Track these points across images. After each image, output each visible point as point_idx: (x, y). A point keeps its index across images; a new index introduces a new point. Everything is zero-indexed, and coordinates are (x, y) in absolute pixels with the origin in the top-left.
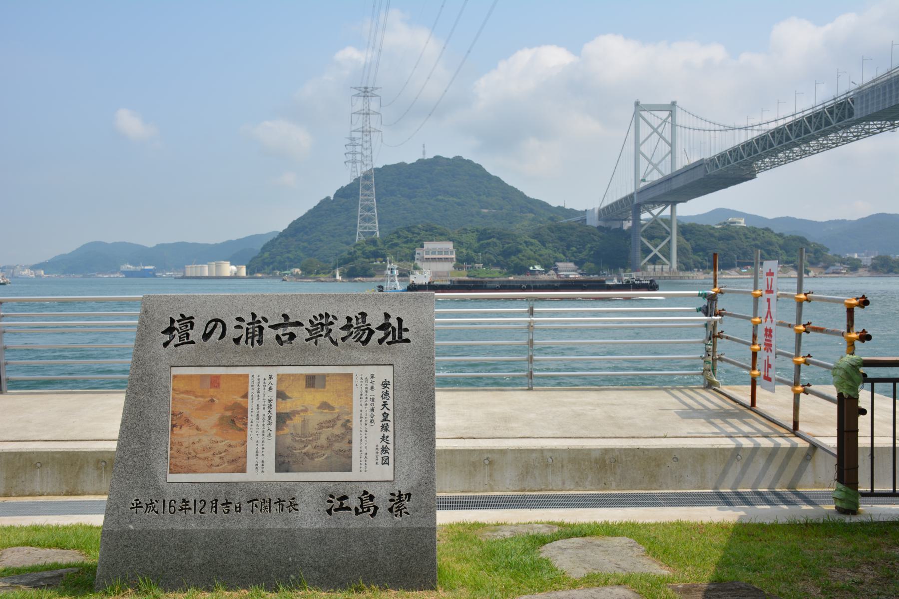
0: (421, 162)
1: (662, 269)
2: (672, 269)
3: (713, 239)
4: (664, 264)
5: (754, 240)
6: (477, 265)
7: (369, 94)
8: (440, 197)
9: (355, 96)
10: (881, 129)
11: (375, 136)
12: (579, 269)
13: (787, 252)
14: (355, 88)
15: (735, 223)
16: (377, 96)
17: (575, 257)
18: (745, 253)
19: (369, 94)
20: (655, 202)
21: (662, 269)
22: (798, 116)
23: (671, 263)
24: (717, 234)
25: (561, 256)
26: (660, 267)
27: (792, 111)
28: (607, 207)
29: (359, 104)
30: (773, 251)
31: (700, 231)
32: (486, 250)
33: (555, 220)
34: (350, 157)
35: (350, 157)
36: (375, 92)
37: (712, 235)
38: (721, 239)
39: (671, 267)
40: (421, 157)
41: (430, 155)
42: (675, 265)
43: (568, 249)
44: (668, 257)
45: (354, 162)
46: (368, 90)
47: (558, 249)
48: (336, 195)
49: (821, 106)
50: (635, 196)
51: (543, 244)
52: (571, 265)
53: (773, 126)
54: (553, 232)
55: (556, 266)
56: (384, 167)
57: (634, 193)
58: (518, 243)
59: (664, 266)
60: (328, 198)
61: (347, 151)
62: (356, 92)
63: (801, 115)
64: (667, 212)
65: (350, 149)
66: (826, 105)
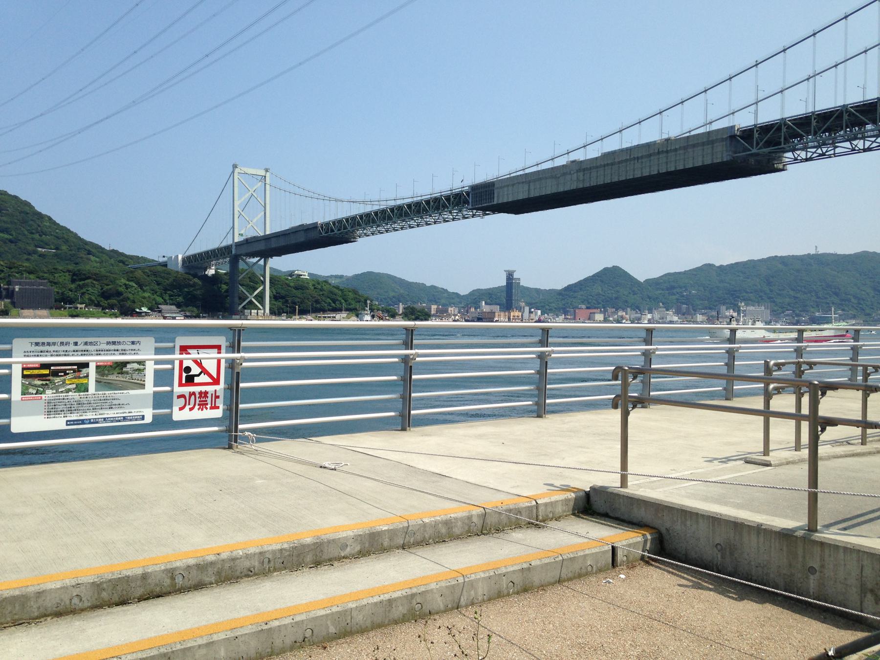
1: (257, 313)
2: (266, 314)
3: (290, 288)
4: (260, 309)
5: (321, 290)
6: (79, 306)
10: (473, 216)
12: (180, 311)
13: (346, 301)
15: (301, 275)
17: (172, 299)
18: (317, 302)
20: (253, 255)
21: (257, 313)
22: (415, 199)
24: (292, 284)
25: (160, 300)
26: (256, 311)
27: (410, 194)
28: (194, 256)
30: (337, 300)
31: (278, 281)
32: (84, 290)
33: (126, 263)
37: (289, 286)
38: (296, 288)
39: (265, 312)
43: (166, 293)
44: (262, 303)
47: (156, 293)
49: (439, 194)
50: (234, 247)
51: (141, 286)
52: (174, 307)
53: (392, 203)
54: (148, 276)
57: (231, 245)
58: (117, 285)
63: (419, 198)
64: (262, 262)
66: (442, 194)
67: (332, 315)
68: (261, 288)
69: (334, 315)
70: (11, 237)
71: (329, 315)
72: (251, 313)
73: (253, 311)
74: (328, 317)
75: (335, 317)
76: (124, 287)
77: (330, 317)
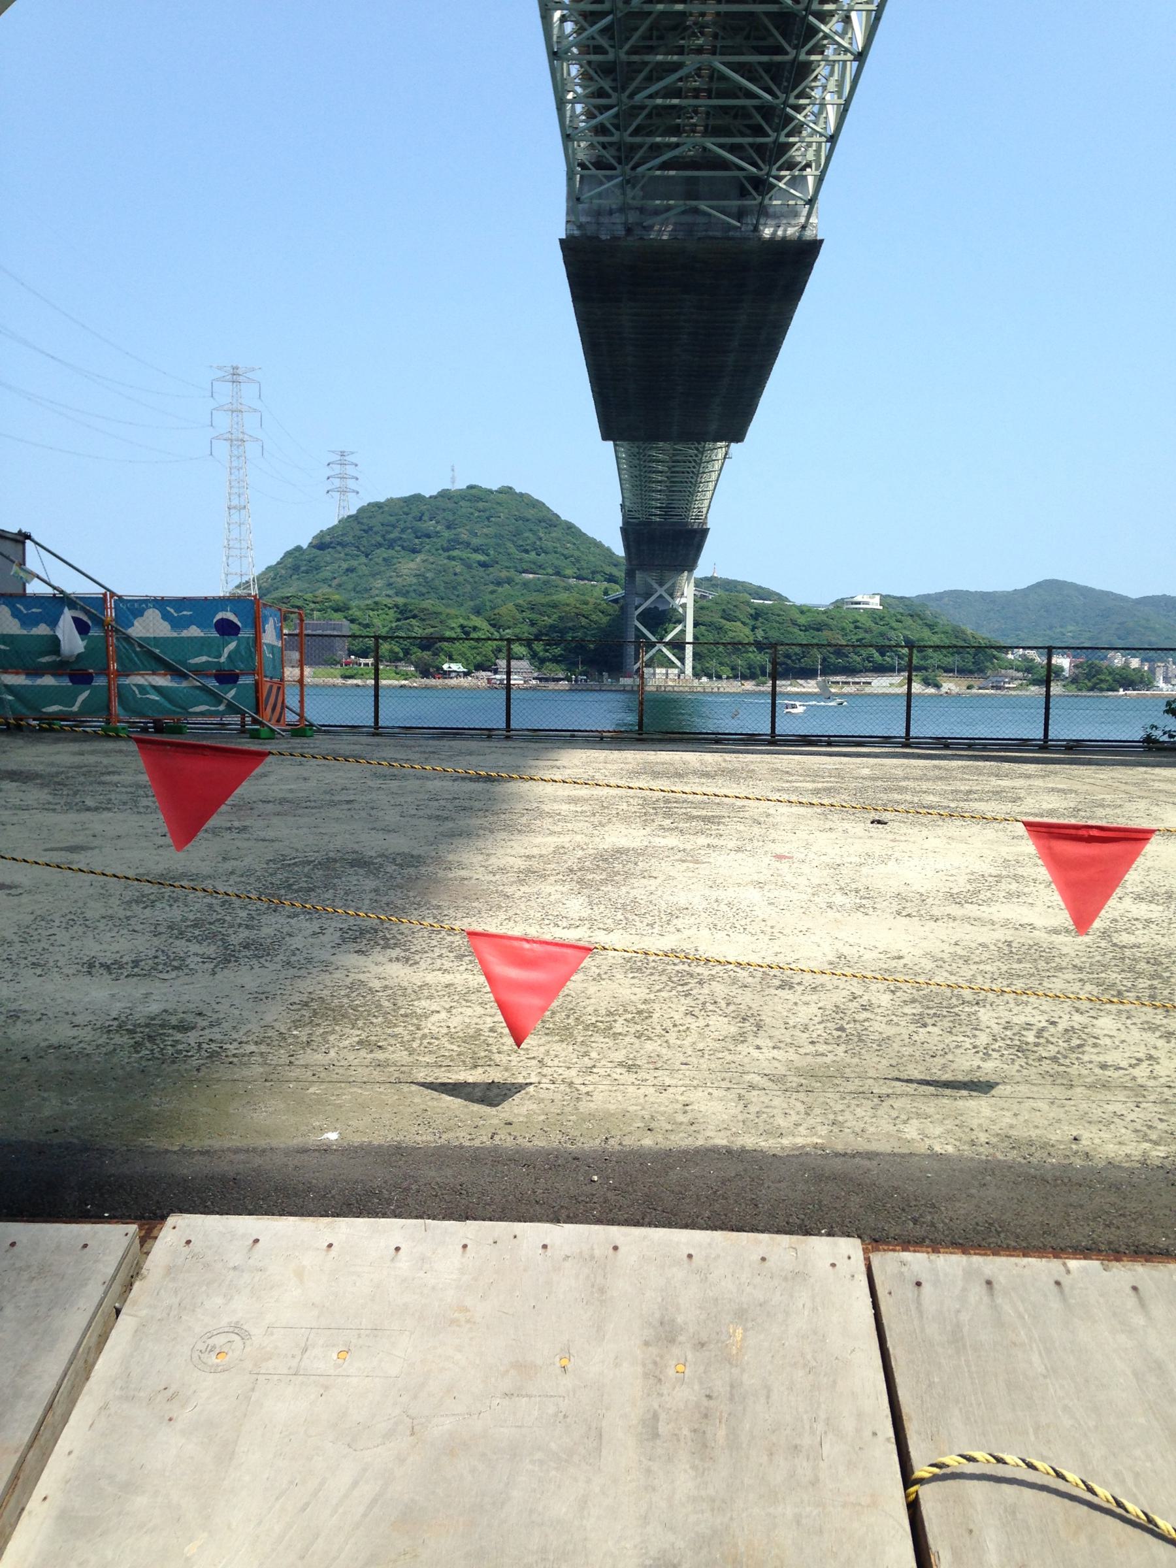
0: (444, 495)
7: (241, 379)
8: (455, 553)
9: (217, 380)
11: (251, 449)
14: (219, 368)
16: (253, 381)
19: (241, 379)
23: (683, 663)
26: (663, 671)
29: (225, 390)
34: (337, 482)
35: (337, 482)
36: (249, 375)
40: (447, 486)
41: (461, 485)
42: (689, 670)
45: (343, 491)
46: (239, 371)
48: (311, 545)
55: (496, 665)
56: (388, 500)
59: (670, 671)
60: (298, 549)
61: (332, 473)
62: (220, 374)
65: (337, 469)
67: (863, 680)
68: (679, 627)
69: (868, 680)
70: (487, 558)
71: (857, 680)
72: (654, 674)
73: (658, 670)
74: (854, 683)
75: (870, 683)
76: (459, 630)
77: (858, 683)
